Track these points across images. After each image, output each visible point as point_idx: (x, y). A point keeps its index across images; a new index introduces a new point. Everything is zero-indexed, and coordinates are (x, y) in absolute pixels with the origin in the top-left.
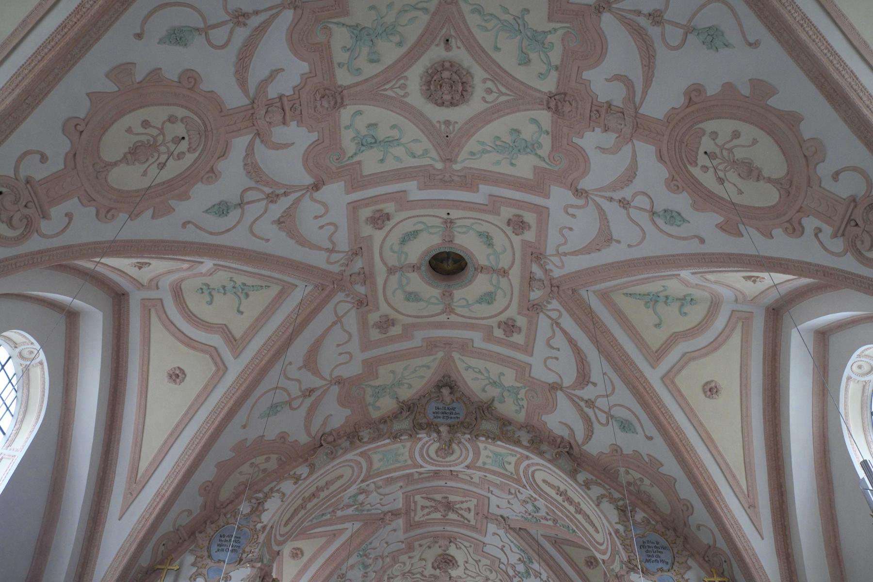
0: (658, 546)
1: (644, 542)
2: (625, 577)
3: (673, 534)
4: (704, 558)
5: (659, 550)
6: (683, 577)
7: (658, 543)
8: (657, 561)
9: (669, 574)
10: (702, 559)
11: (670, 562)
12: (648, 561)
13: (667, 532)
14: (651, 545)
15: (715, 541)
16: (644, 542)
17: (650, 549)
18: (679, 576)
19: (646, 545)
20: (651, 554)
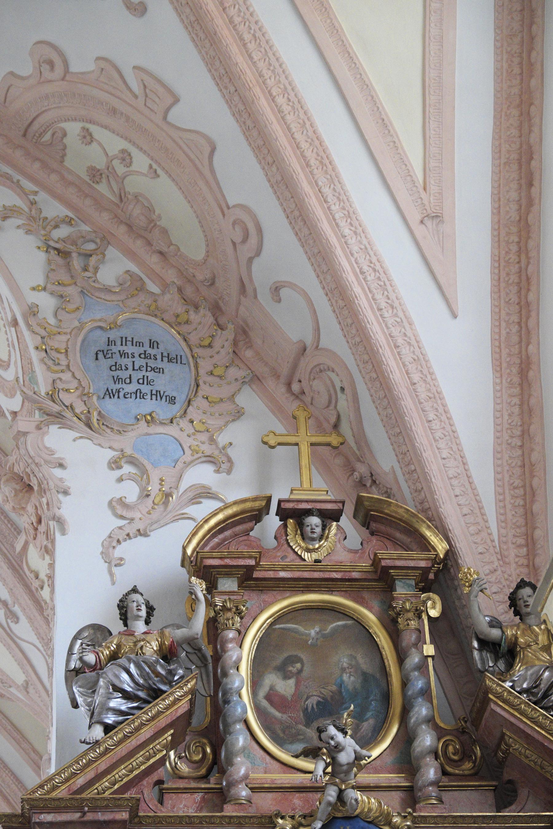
0: (150, 351)
1: (110, 342)
2: (30, 438)
3: (210, 319)
4: (289, 385)
5: (152, 363)
6: (212, 441)
7: (153, 344)
8: (139, 394)
9: (173, 430)
10: (283, 389)
11: (181, 398)
12: (110, 394)
13: (192, 316)
14: (129, 349)
15: (317, 330)
16: (110, 342)
17: (128, 361)
18: (204, 437)
19: (115, 349)
20: (124, 375)
